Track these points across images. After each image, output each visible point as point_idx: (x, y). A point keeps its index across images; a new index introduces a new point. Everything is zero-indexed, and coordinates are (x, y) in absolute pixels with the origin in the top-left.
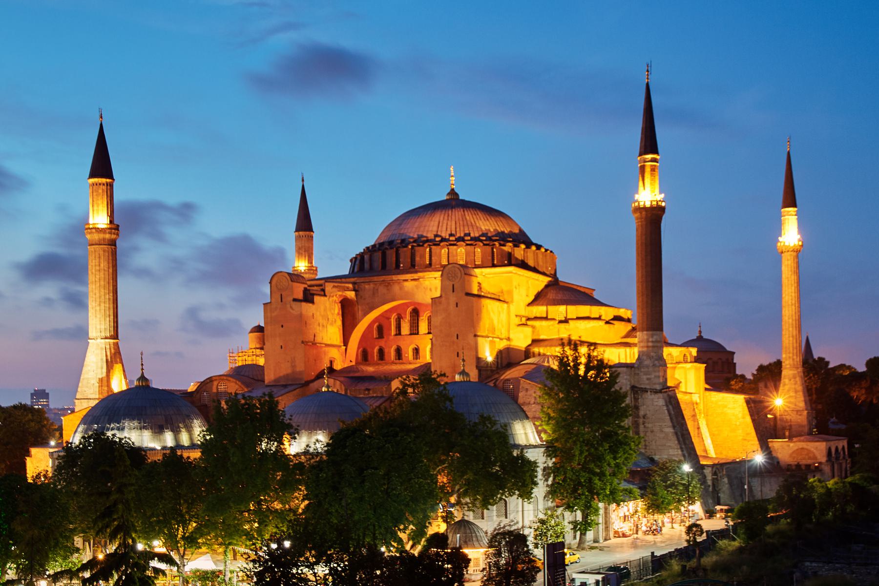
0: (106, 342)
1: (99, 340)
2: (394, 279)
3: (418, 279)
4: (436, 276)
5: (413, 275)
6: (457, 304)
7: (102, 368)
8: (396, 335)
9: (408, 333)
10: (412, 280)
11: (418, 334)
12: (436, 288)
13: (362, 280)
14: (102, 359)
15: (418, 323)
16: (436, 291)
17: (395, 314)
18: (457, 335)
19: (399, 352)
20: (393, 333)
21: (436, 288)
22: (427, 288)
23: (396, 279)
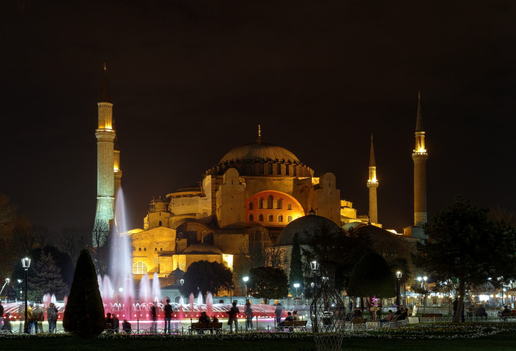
0: (111, 199)
1: (108, 198)
2: (267, 179)
3: (281, 180)
4: (291, 179)
5: (278, 178)
6: (331, 193)
7: (111, 214)
8: (260, 208)
9: (267, 208)
10: (278, 180)
11: (272, 208)
12: (290, 185)
13: (249, 177)
14: (111, 209)
15: (272, 203)
16: (290, 187)
17: (260, 197)
18: (331, 208)
19: (261, 217)
20: (259, 207)
21: (290, 185)
22: (286, 185)
23: (269, 179)
